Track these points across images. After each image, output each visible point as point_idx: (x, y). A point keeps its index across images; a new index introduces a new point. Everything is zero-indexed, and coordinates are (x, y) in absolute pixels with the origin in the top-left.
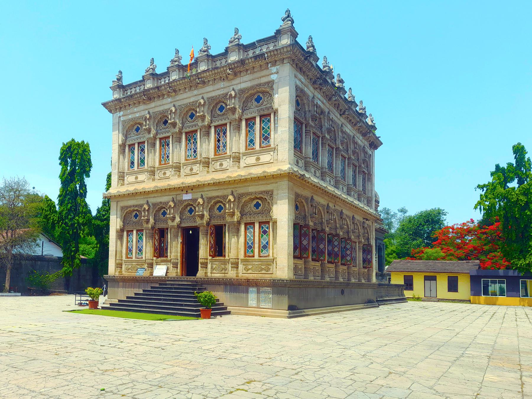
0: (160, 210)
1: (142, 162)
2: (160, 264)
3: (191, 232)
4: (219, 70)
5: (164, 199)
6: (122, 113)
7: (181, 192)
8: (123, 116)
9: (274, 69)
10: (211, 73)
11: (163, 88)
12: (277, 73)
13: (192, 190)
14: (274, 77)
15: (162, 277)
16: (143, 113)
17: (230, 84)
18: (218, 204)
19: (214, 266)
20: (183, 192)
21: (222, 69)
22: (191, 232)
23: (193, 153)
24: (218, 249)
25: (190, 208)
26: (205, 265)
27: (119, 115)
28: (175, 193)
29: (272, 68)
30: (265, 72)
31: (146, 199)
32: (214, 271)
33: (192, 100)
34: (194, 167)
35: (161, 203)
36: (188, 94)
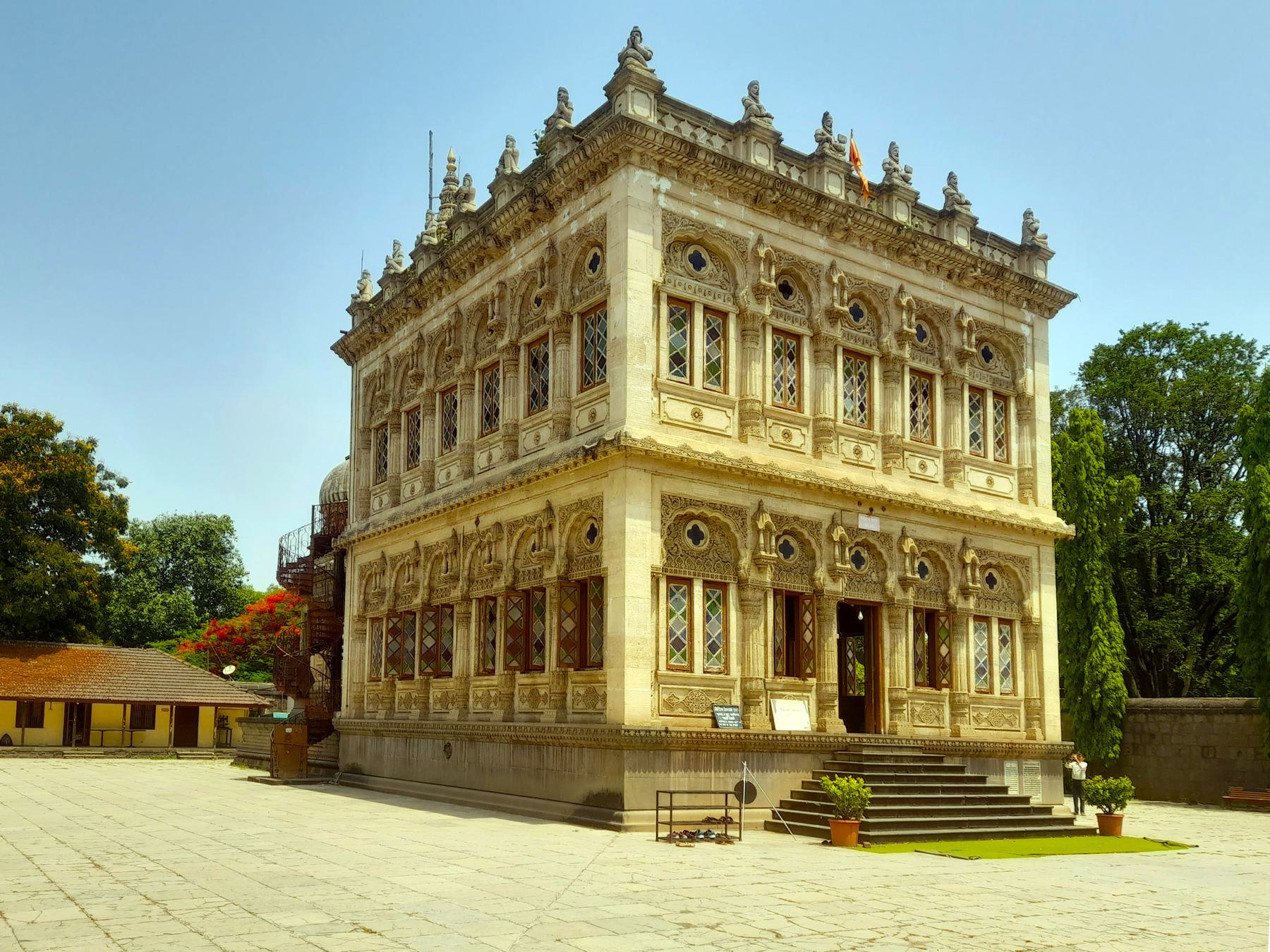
0: (792, 540)
1: (715, 370)
2: (781, 697)
3: (861, 616)
4: (958, 257)
5: (809, 511)
6: (665, 184)
7: (857, 507)
8: (668, 194)
9: (1029, 317)
10: (942, 250)
11: (832, 207)
12: (1031, 326)
13: (884, 509)
14: (1025, 330)
15: (802, 736)
16: (739, 230)
17: (957, 295)
18: (932, 559)
19: (918, 709)
20: (861, 509)
21: (964, 258)
22: (861, 616)
23: (858, 409)
24: (934, 670)
25: (864, 551)
26: (896, 703)
27: (654, 183)
28: (841, 505)
29: (1026, 312)
30: (1011, 311)
31: (758, 497)
32: (917, 722)
33: (876, 278)
34: (864, 448)
35: (796, 519)
36: (867, 258)
